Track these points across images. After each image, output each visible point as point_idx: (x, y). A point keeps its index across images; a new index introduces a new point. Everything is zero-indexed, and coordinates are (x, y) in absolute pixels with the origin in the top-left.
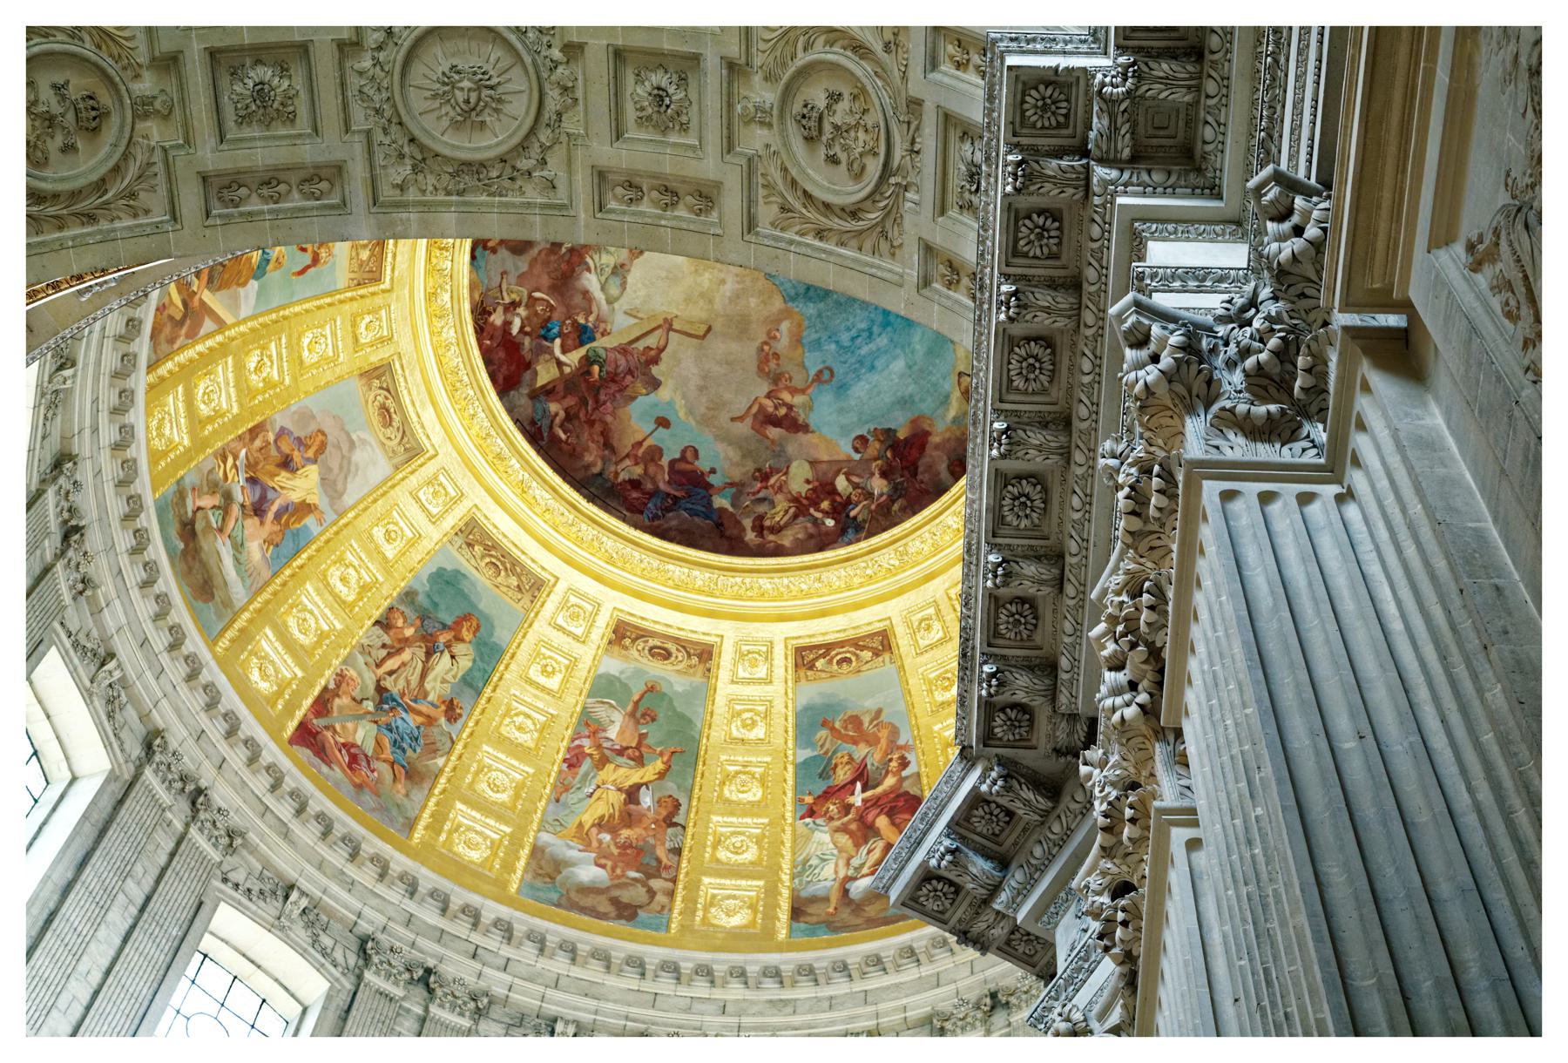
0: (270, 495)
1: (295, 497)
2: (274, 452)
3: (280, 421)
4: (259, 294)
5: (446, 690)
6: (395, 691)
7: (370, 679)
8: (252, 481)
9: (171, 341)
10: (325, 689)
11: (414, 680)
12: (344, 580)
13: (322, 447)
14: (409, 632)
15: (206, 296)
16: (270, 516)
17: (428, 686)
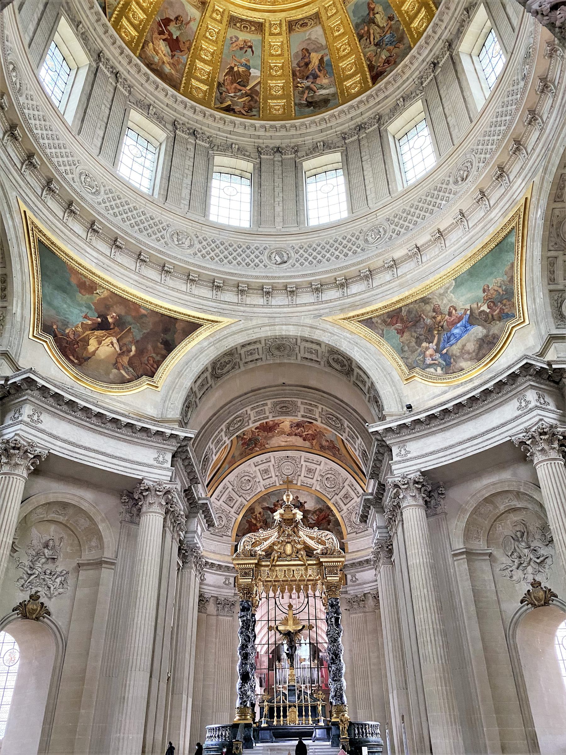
0: (313, 72)
1: (317, 63)
2: (302, 69)
3: (295, 65)
4: (255, 68)
5: (386, 18)
6: (379, 39)
7: (373, 47)
8: (307, 77)
9: (256, 101)
10: (368, 65)
11: (379, 30)
12: (343, 51)
13: (307, 50)
14: (366, 28)
15: (248, 88)
16: (319, 73)
17: (382, 26)
